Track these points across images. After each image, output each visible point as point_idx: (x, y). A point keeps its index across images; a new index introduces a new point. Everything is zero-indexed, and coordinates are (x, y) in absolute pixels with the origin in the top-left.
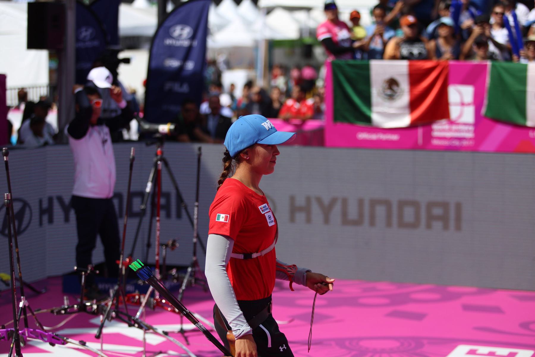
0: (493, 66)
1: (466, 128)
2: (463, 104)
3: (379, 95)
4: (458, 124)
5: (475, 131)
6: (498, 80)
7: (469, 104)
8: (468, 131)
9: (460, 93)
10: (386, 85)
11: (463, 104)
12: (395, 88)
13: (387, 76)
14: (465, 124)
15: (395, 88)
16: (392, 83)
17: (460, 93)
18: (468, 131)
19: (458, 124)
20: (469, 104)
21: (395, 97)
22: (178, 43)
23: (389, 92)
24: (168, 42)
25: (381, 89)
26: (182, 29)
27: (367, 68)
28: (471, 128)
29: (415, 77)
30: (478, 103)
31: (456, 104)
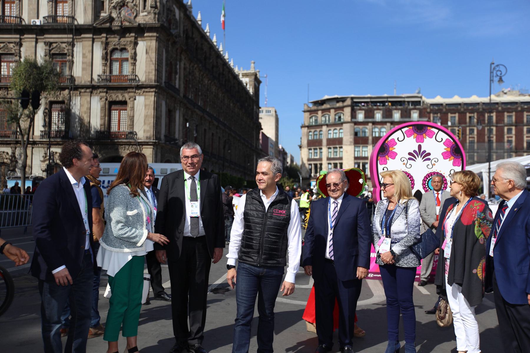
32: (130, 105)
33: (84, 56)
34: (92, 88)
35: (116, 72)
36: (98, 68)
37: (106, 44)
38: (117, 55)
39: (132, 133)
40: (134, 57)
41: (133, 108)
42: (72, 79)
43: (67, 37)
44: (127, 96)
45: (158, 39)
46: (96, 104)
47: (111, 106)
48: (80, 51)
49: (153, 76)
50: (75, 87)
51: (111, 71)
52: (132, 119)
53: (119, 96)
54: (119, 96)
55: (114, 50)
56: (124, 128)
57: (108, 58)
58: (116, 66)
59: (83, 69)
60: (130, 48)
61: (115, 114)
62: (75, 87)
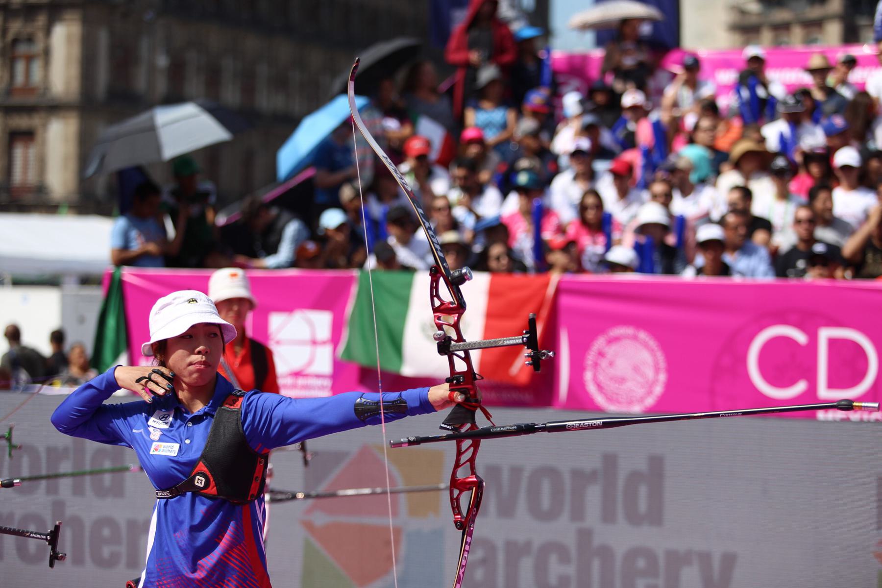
2: (314, 343)
4: (306, 376)
7: (324, 343)
8: (322, 388)
11: (314, 343)
14: (318, 376)
17: (311, 324)
18: (322, 388)
19: (306, 376)
20: (324, 343)
28: (328, 383)
32: (39, 138)
35: (20, 79)
38: (22, 49)
39: (41, 189)
40: (47, 53)
41: (44, 143)
44: (35, 121)
45: (86, 22)
49: (74, 87)
51: (12, 76)
52: (42, 162)
53: (21, 122)
54: (21, 122)
55: (15, 41)
56: (32, 178)
58: (20, 67)
60: (40, 35)
61: (19, 152)
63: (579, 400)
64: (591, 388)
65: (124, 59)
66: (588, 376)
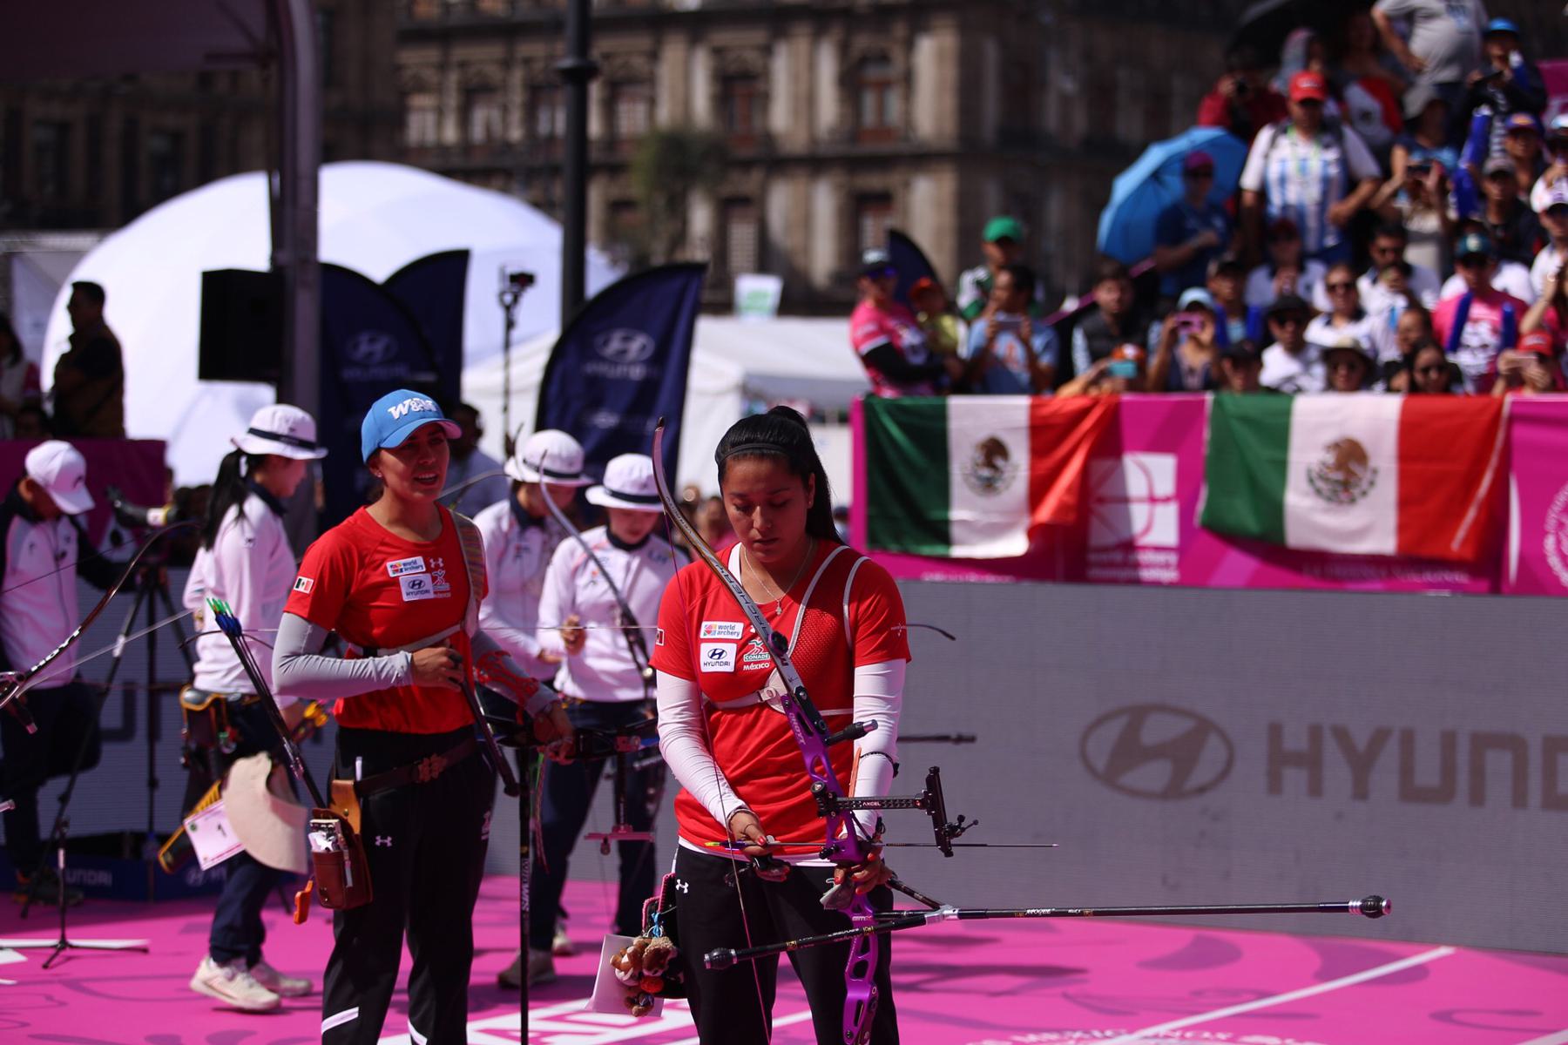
0: (1217, 403)
1: (1160, 558)
2: (1153, 500)
3: (966, 478)
5: (1181, 566)
6: (1225, 440)
7: (1167, 500)
8: (1166, 566)
9: (1146, 471)
10: (980, 458)
11: (1153, 500)
12: (999, 462)
13: (982, 435)
15: (999, 462)
16: (994, 450)
17: (1146, 471)
20: (1167, 500)
21: (999, 484)
22: (618, 371)
23: (986, 472)
24: (591, 368)
25: (969, 465)
26: (627, 339)
27: (941, 415)
28: (1173, 558)
29: (1046, 435)
30: (1185, 496)
31: (1140, 500)
33: (795, 78)
34: (814, 163)
35: (869, 118)
36: (829, 109)
37: (844, 49)
38: (873, 73)
40: (908, 80)
41: (906, 212)
42: (769, 138)
43: (757, 36)
45: (966, 32)
46: (825, 200)
47: (858, 206)
48: (783, 68)
49: (950, 126)
50: (778, 162)
53: (873, 181)
54: (873, 181)
55: (864, 60)
57: (851, 83)
58: (869, 100)
59: (795, 112)
60: (897, 54)
62: (777, 163)
63: (1537, 580)
64: (1554, 561)
65: (1023, 84)
66: (1550, 543)
